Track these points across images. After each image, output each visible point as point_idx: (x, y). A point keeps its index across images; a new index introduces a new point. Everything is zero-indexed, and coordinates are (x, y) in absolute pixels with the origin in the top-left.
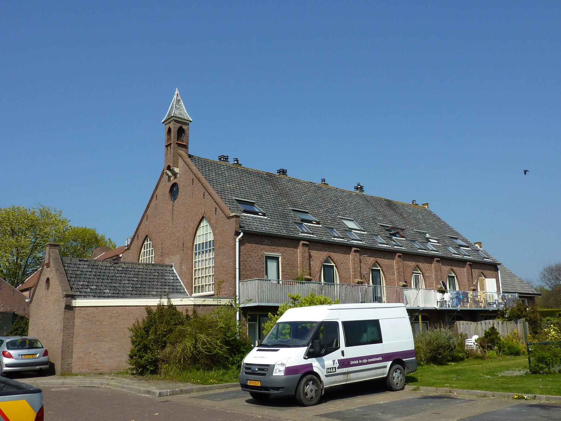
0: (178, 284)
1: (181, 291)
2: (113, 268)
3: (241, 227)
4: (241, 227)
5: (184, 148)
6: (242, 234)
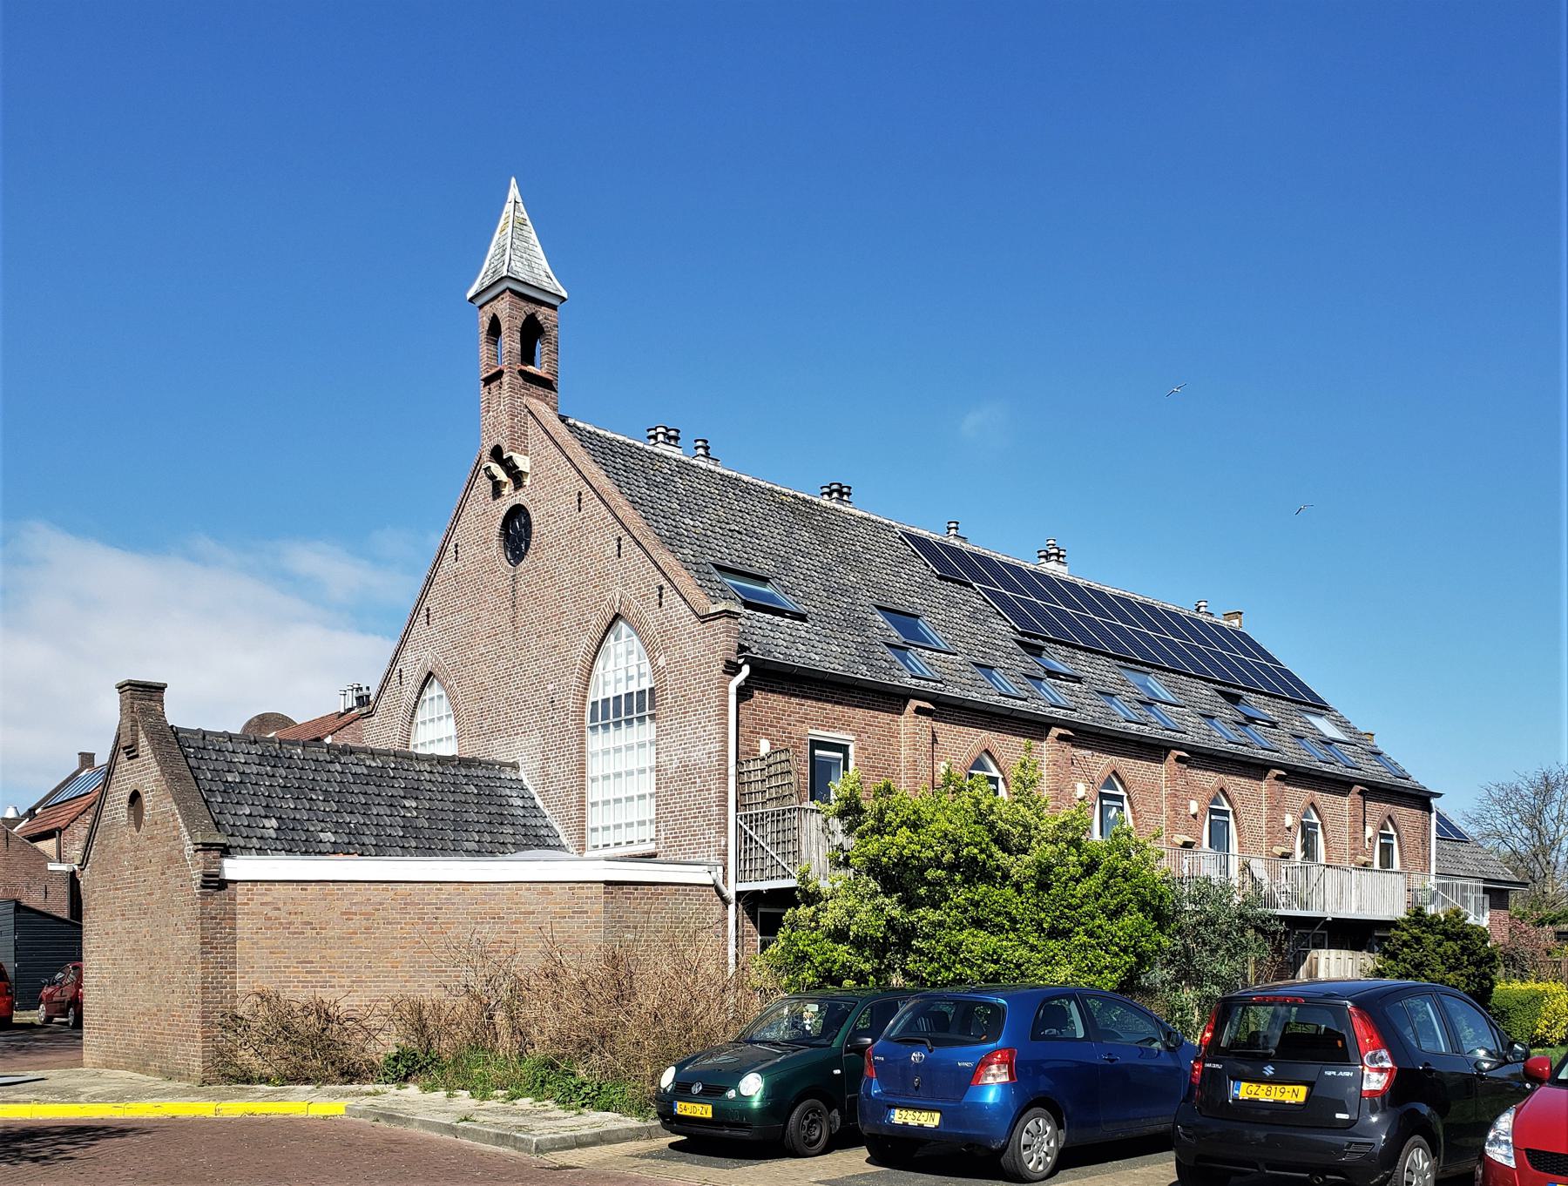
0: (540, 822)
1: (551, 842)
2: (338, 767)
3: (742, 648)
4: (742, 648)
5: (541, 391)
6: (746, 670)
